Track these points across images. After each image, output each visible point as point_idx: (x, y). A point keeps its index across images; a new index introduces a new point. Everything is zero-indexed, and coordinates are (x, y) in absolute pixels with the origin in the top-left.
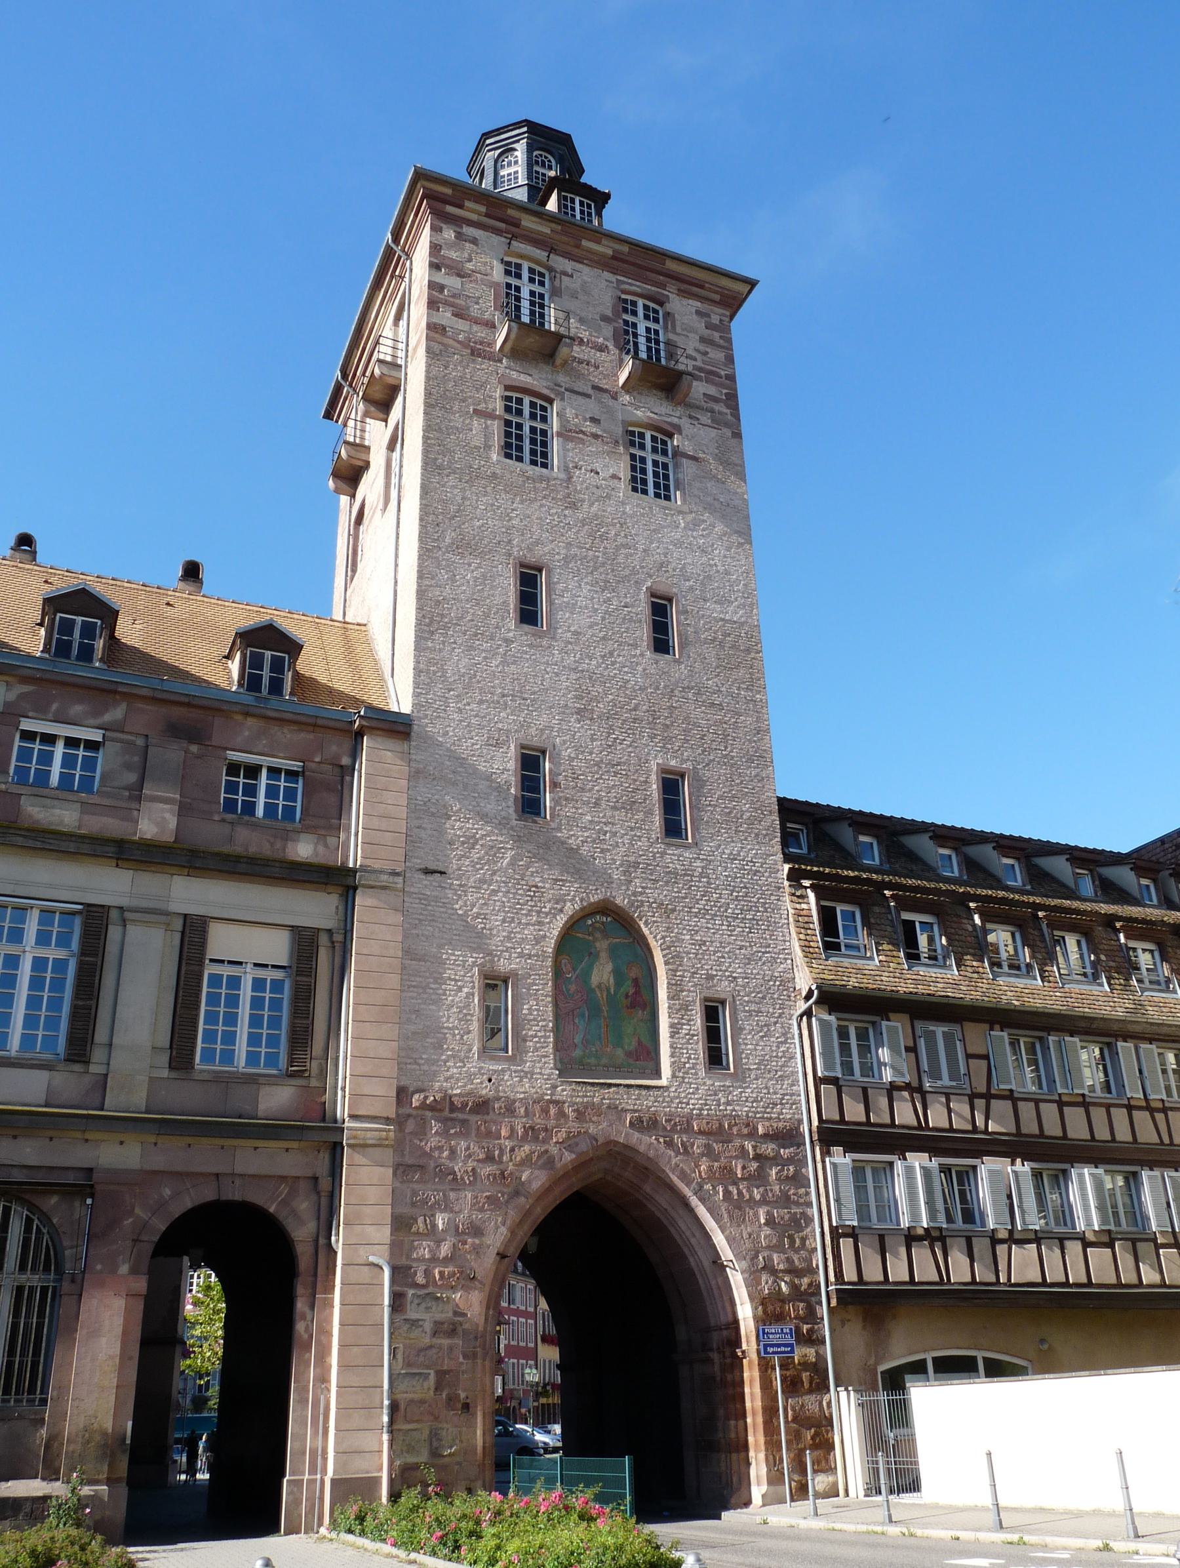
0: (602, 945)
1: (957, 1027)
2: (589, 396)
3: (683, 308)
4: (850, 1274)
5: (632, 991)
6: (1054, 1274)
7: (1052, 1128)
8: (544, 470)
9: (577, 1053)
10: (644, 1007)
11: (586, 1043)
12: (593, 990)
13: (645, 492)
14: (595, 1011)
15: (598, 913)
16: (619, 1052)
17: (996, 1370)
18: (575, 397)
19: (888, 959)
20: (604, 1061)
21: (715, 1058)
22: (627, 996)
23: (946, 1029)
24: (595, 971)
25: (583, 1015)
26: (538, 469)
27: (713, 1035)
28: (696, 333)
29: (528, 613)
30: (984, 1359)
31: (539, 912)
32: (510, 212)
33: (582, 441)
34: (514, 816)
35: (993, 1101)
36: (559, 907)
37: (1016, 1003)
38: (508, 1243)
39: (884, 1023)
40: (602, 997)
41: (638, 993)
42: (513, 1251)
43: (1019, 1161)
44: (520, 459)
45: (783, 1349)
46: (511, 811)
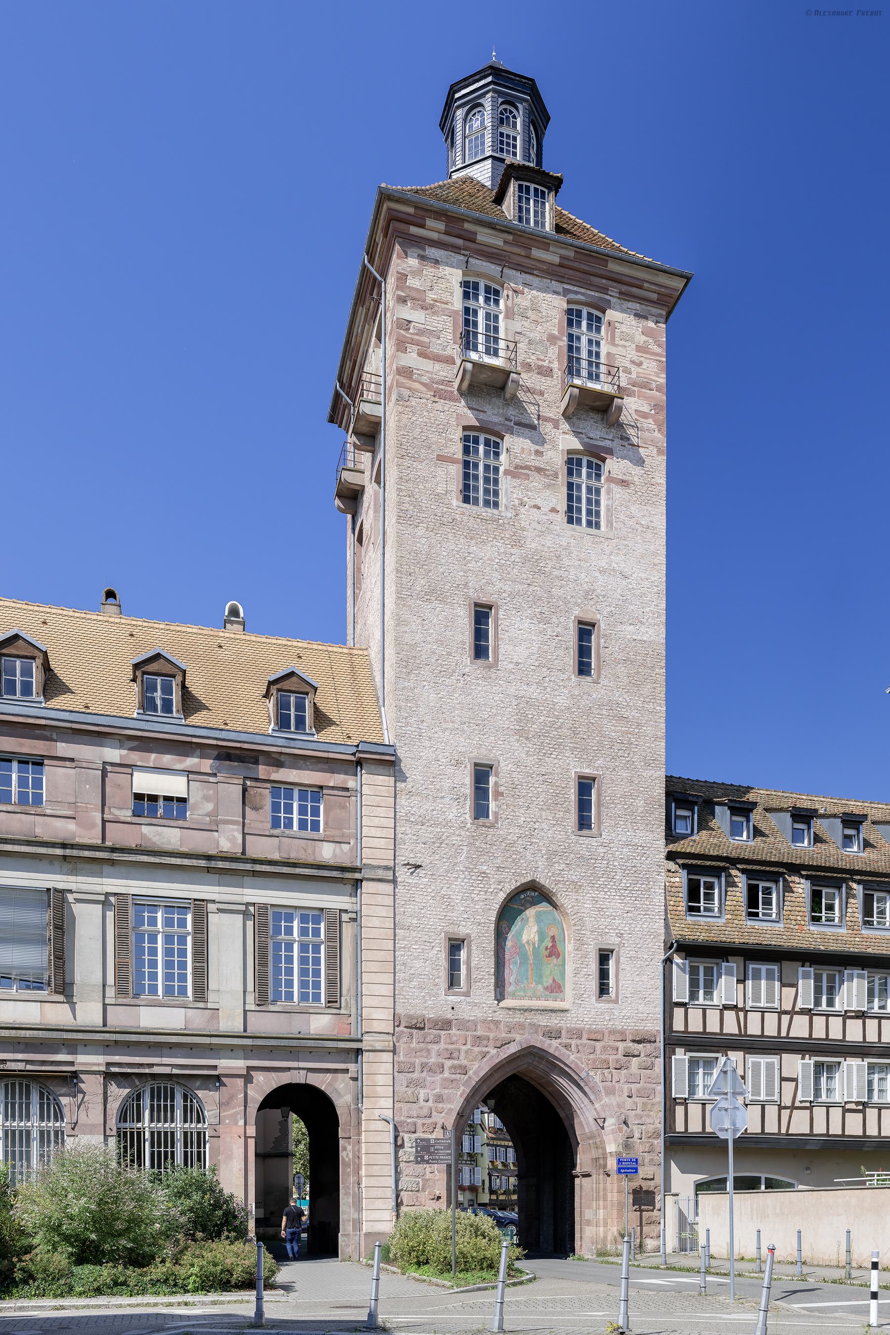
4: (680, 1127)
5: (550, 945)
7: (836, 1033)
8: (495, 511)
10: (558, 956)
11: (517, 982)
13: (579, 521)
16: (540, 987)
17: (771, 1185)
19: (734, 917)
20: (530, 993)
21: (603, 989)
22: (547, 948)
25: (516, 963)
26: (491, 511)
27: (604, 974)
31: (486, 892)
32: (467, 226)
33: (527, 477)
34: (469, 820)
36: (500, 887)
37: (822, 948)
40: (529, 949)
41: (554, 946)
44: (476, 502)
46: (467, 816)
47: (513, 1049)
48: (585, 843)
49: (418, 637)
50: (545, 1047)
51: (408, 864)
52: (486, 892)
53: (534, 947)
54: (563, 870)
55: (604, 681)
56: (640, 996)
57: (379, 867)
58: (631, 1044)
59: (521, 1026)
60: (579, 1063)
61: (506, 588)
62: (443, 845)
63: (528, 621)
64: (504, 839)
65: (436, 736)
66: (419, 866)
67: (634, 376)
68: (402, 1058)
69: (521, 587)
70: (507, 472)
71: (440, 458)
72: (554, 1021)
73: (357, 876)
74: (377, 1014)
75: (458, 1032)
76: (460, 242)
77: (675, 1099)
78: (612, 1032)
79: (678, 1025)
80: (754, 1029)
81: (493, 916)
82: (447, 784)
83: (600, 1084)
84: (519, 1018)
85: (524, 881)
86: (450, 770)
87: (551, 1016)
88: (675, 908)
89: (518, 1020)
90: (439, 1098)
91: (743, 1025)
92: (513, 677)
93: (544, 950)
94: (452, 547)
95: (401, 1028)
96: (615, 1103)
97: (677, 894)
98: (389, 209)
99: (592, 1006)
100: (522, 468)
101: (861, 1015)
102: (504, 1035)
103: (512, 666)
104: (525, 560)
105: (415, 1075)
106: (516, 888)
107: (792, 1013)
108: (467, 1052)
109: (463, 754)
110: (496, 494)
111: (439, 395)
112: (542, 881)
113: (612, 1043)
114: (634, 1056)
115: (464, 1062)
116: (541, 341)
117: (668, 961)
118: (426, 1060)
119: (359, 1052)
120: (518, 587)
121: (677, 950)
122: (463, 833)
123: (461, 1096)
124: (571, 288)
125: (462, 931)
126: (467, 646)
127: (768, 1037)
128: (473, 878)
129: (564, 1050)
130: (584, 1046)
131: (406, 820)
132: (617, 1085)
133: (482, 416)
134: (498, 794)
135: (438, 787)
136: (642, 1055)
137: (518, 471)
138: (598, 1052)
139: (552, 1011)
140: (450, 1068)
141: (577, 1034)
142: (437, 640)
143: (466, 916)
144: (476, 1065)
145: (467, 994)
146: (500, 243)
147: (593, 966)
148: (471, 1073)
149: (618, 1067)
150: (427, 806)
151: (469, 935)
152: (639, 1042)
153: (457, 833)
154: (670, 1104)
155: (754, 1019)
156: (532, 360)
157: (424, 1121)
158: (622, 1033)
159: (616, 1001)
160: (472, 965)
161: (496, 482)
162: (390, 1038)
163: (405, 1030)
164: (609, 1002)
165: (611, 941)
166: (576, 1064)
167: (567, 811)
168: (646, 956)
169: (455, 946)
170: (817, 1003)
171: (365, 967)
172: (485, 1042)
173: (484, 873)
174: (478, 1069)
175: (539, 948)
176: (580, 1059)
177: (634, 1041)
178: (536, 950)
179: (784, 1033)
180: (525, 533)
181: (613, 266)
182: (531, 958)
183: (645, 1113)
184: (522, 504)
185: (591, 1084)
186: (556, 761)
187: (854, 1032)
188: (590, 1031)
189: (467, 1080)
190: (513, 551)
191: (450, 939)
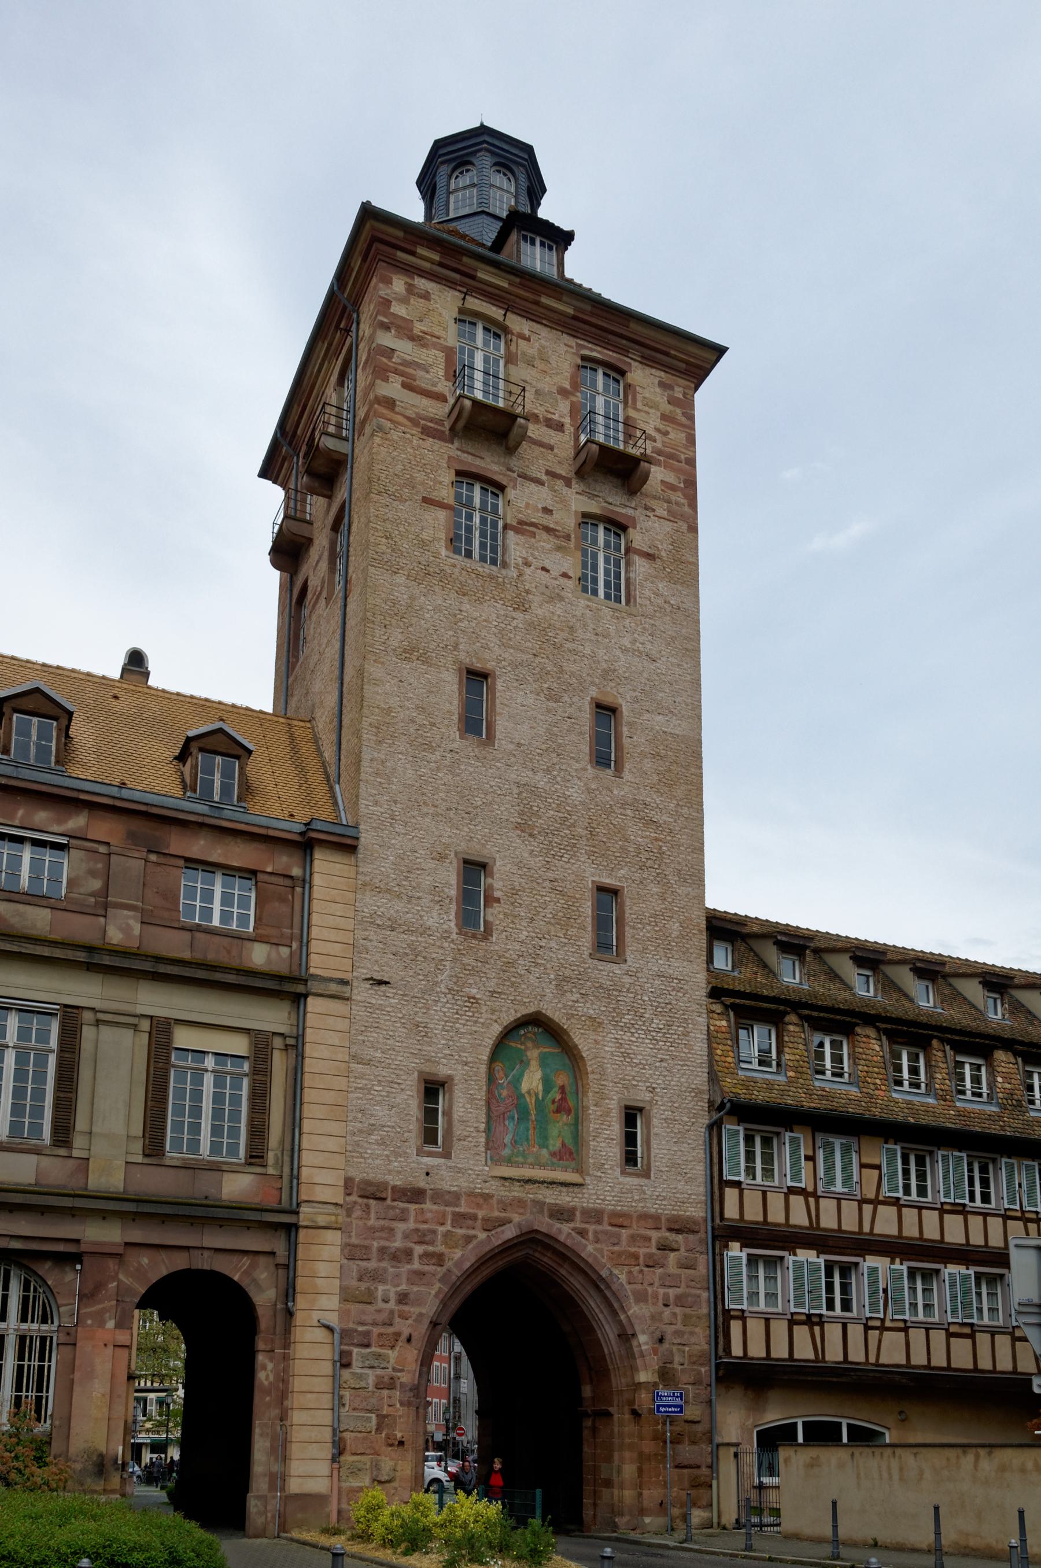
0: (533, 1054)
1: (855, 1140)
2: (542, 484)
3: (640, 376)
4: (737, 1350)
5: (558, 1097)
6: (919, 1358)
7: (931, 1233)
9: (506, 1152)
10: (569, 1112)
11: (514, 1143)
12: (523, 1096)
16: (544, 1152)
18: (528, 483)
20: (531, 1160)
21: (630, 1159)
22: (553, 1102)
23: (844, 1141)
25: (513, 1118)
27: (630, 1139)
28: (655, 406)
29: (474, 722)
30: (848, 1425)
33: (533, 535)
34: (455, 930)
35: (881, 1208)
37: (912, 1120)
38: (439, 1313)
39: (788, 1134)
40: (531, 1102)
41: (563, 1099)
42: (445, 1319)
43: (898, 1260)
45: (673, 1409)
46: (453, 924)
47: (509, 1233)
48: (606, 971)
49: (394, 702)
50: (553, 1232)
51: (371, 979)
52: (476, 1022)
55: (627, 775)
56: (676, 1176)
57: (331, 980)
58: (668, 1234)
59: (521, 1203)
60: (599, 1256)
61: (506, 655)
62: (419, 958)
63: (533, 696)
64: (500, 957)
65: (414, 821)
66: (387, 983)
67: (659, 445)
68: (354, 1240)
69: (525, 657)
70: (506, 527)
71: (426, 500)
72: (565, 1198)
73: (300, 989)
74: (320, 1177)
75: (435, 1207)
76: (457, 276)
77: (729, 1310)
78: (644, 1217)
79: (731, 1212)
80: (828, 1221)
82: (427, 881)
83: (627, 1287)
84: (517, 1192)
86: (431, 865)
87: (560, 1191)
88: (723, 1058)
89: (516, 1194)
90: (403, 1298)
91: (814, 1216)
92: (513, 759)
93: (550, 1104)
94: (439, 602)
95: (354, 1198)
96: (648, 1314)
97: (724, 1042)
98: (373, 228)
99: (615, 1181)
100: (526, 524)
101: (960, 1210)
102: (496, 1214)
103: (512, 747)
104: (531, 626)
105: (372, 1264)
106: (515, 1020)
107: (876, 1202)
108: (447, 1235)
109: (447, 846)
110: (494, 550)
111: (427, 432)
112: (549, 1014)
113: (643, 1232)
114: (673, 1250)
115: (440, 1248)
116: (550, 393)
117: (715, 1128)
118: (387, 1244)
119: (296, 1227)
120: (520, 656)
121: (728, 1113)
122: (446, 945)
123: (436, 1295)
124: (586, 344)
125: (443, 1071)
126: (455, 718)
127: (846, 1232)
128: (459, 1003)
129: (578, 1238)
130: (605, 1233)
131: (372, 923)
132: (650, 1290)
133: (478, 462)
134: (490, 900)
135: (414, 884)
136: (683, 1249)
137: (523, 527)
138: (624, 1243)
139: (563, 1184)
140: (420, 1257)
141: (595, 1215)
142: (418, 707)
143: (447, 1052)
144: (458, 1254)
145: (447, 1155)
146: (506, 285)
147: (616, 1128)
148: (449, 1264)
149: (651, 1264)
150: (399, 905)
151: (450, 1078)
152: (678, 1231)
153: (438, 944)
154: (723, 1319)
155: (828, 1206)
156: (540, 411)
157: (382, 1330)
158: (656, 1218)
159: (647, 1175)
160: (455, 1116)
161: (494, 538)
162: (339, 1211)
163: (360, 1200)
164: (638, 1176)
165: (641, 1096)
166: (595, 1258)
167: (583, 928)
168: (685, 1119)
169: (432, 1089)
170: (907, 1190)
171: (308, 1110)
172: (470, 1222)
173: (474, 998)
174: (460, 1258)
176: (601, 1251)
177: (670, 1230)
178: (539, 1104)
179: (866, 1229)
180: (530, 596)
181: (633, 325)
182: (533, 1112)
183: (688, 1329)
184: (527, 564)
185: (614, 1287)
186: (568, 866)
187: (954, 1232)
188: (614, 1214)
189: (445, 1275)
190: (514, 614)
191: (426, 1082)
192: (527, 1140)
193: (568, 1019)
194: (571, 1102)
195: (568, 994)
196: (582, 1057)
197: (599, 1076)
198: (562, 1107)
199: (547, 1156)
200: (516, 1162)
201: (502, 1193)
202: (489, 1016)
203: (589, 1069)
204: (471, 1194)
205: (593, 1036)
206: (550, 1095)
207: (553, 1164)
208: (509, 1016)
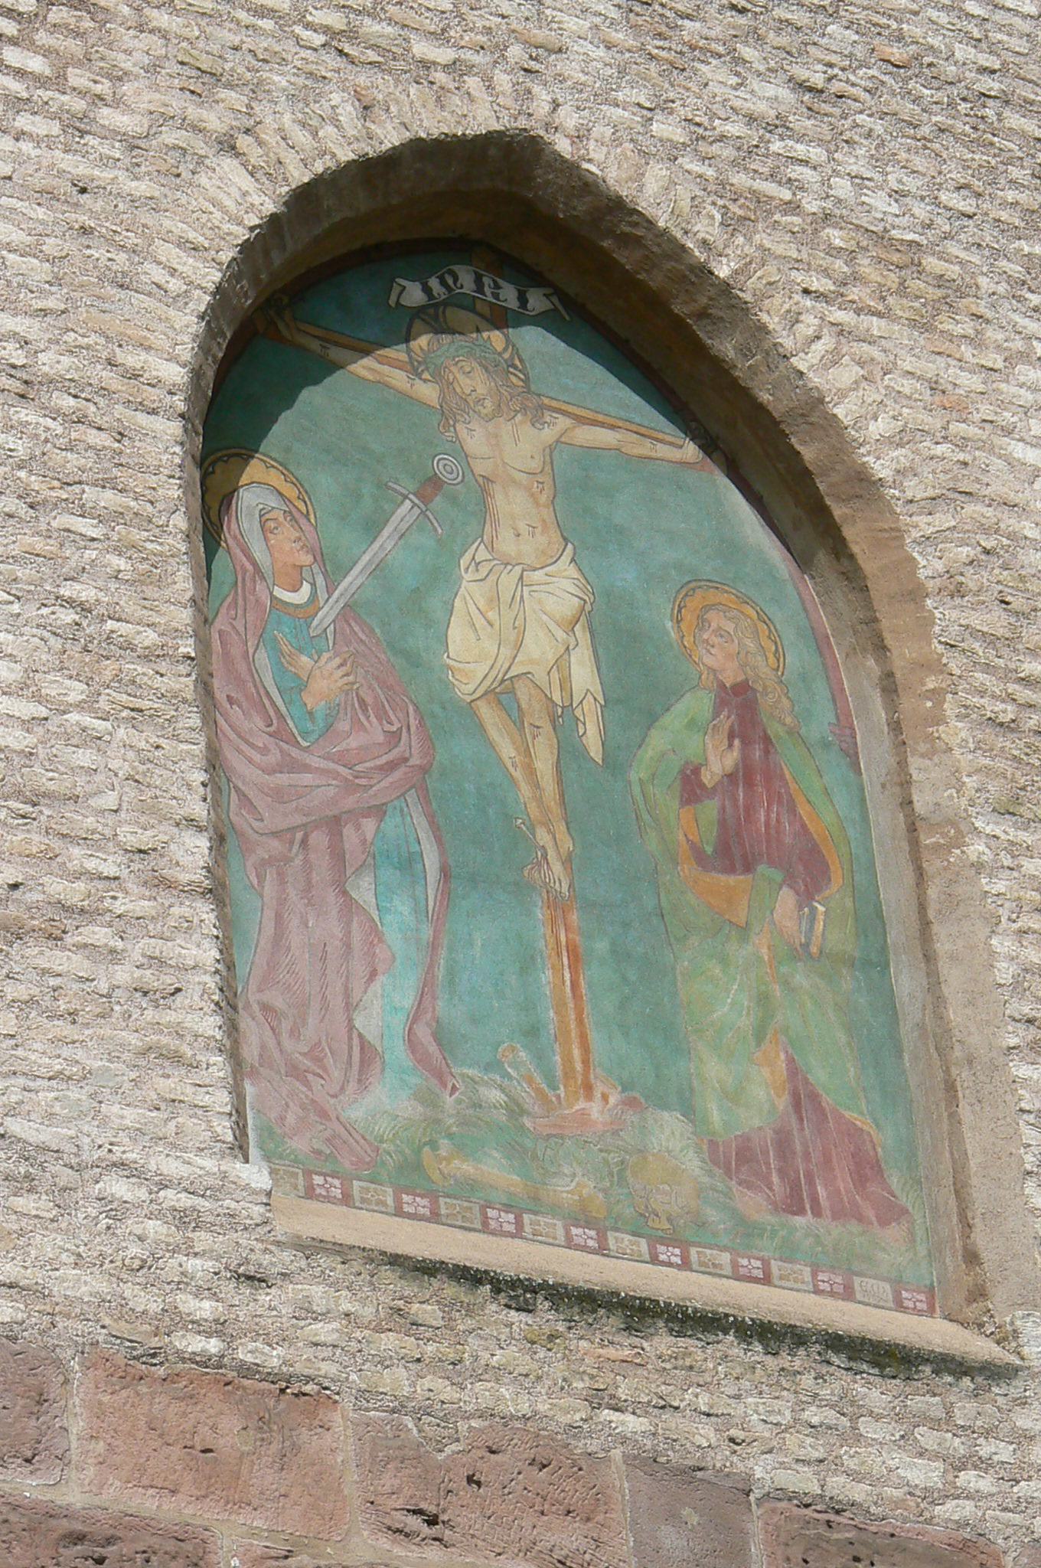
5: (720, 762)
9: (384, 1105)
10: (809, 869)
11: (436, 1050)
14: (481, 856)
15: (457, 247)
16: (669, 1132)
20: (571, 1184)
22: (691, 785)
24: (471, 592)
25: (409, 864)
31: (78, 127)
36: (215, 120)
52: (78, 127)
53: (569, 750)
54: (779, 126)
81: (170, 352)
85: (433, 123)
89: (512, 1400)
93: (668, 802)
112: (607, 165)
175: (615, 762)
182: (553, 841)
192: (532, 1032)
193: (732, 225)
194: (821, 798)
195: (715, 72)
196: (864, 485)
197: (994, 620)
198: (752, 830)
199: (692, 1164)
200: (467, 1188)
201: (397, 1380)
202: (178, 103)
203: (928, 566)
204: (139, 1365)
205: (913, 357)
206: (658, 741)
207: (747, 1231)
208: (340, 132)
